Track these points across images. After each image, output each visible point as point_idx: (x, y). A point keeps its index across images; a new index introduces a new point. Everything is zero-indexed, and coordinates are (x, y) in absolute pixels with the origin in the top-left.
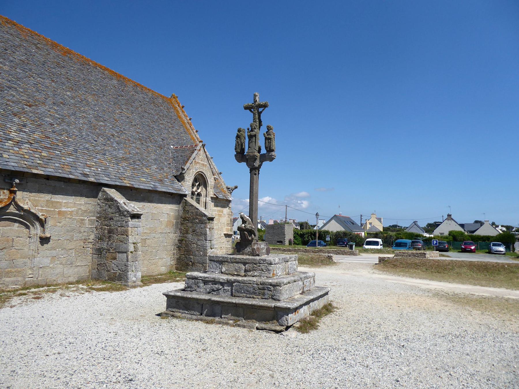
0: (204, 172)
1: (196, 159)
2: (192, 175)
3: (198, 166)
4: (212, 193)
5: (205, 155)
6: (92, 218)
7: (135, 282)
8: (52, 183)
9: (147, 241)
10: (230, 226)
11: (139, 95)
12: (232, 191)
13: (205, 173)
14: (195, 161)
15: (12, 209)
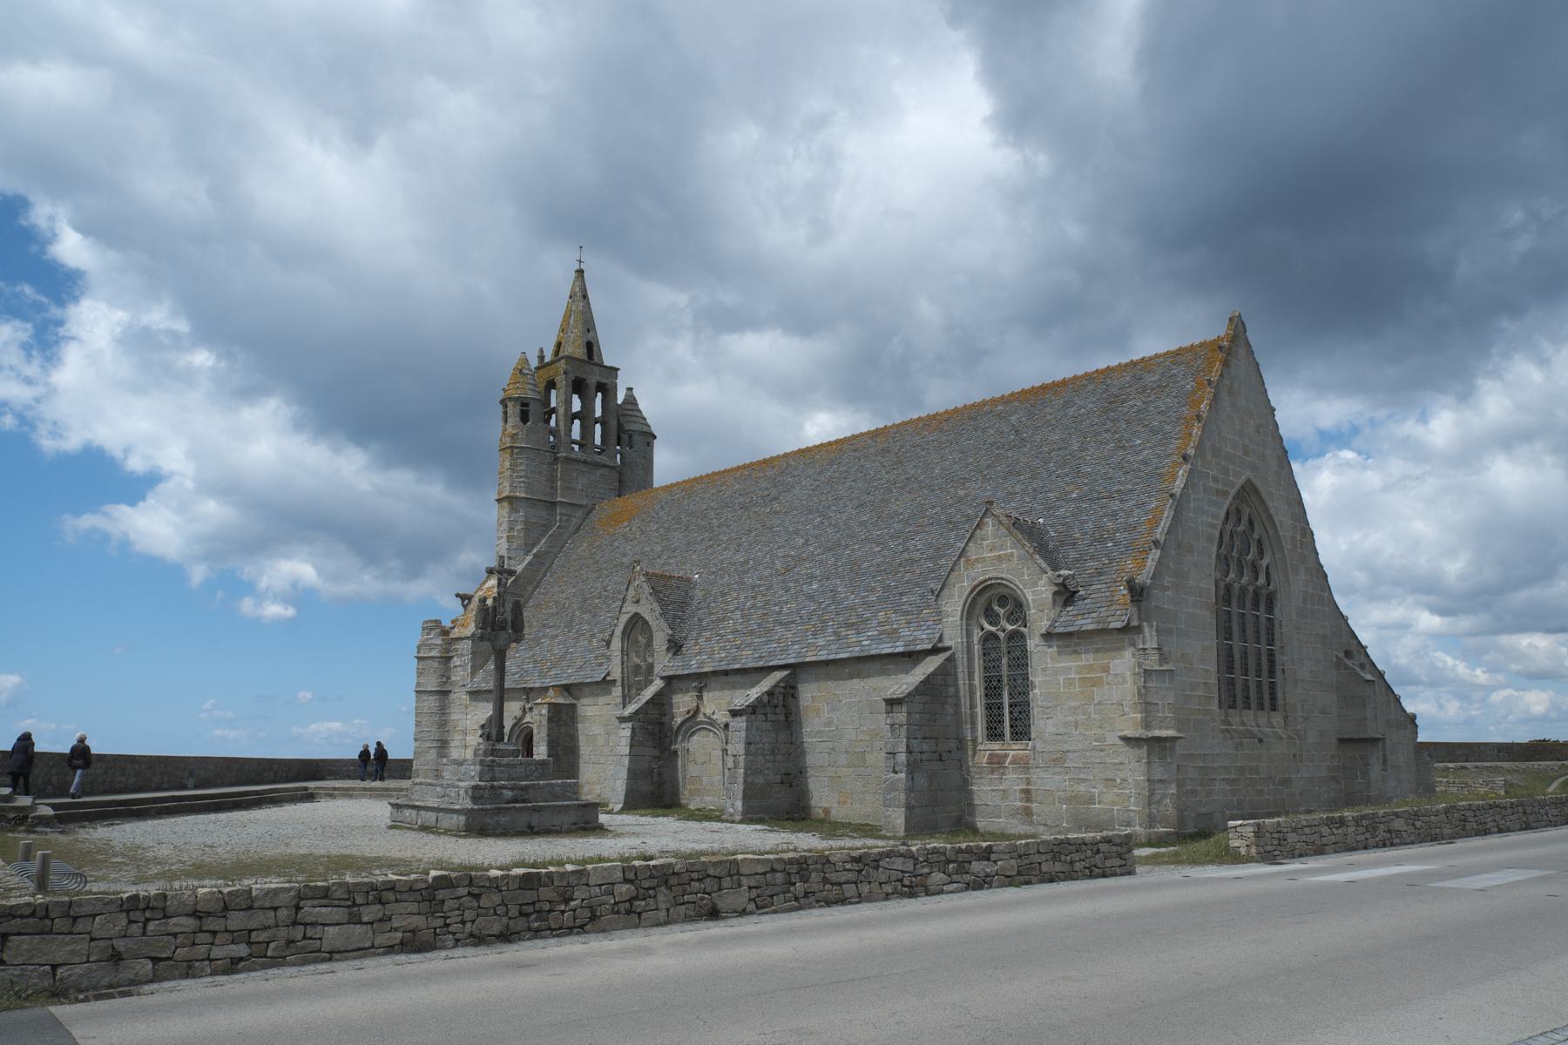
1: (969, 554)
2: (960, 597)
3: (979, 568)
7: (732, 815)
8: (730, 679)
9: (868, 757)
13: (1010, 577)
14: (968, 561)
15: (701, 718)
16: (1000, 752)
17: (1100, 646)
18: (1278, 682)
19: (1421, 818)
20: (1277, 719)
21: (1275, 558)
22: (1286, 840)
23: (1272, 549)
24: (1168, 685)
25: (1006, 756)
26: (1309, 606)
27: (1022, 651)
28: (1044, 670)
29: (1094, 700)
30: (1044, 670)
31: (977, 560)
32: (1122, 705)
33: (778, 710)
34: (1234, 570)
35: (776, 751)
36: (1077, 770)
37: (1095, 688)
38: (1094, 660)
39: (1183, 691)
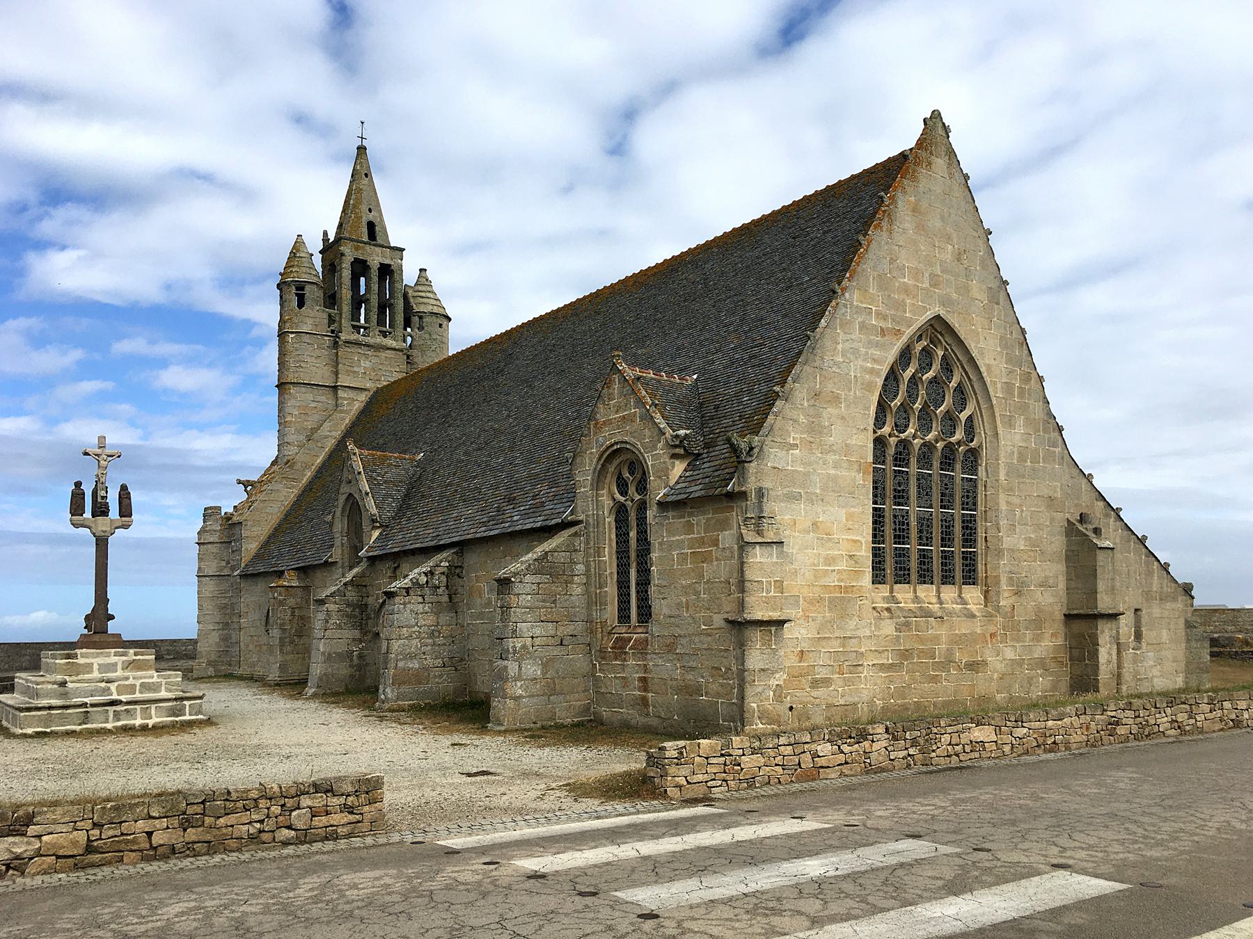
2: (590, 465)
13: (633, 440)
16: (626, 635)
17: (710, 516)
18: (979, 551)
19: (1024, 724)
20: (973, 594)
21: (980, 409)
22: (739, 765)
23: (977, 398)
24: (775, 560)
25: (630, 639)
26: (1029, 464)
28: (660, 544)
33: (440, 591)
34: (914, 424)
35: (436, 634)
36: (687, 658)
37: (705, 565)
38: (705, 533)
39: (814, 565)
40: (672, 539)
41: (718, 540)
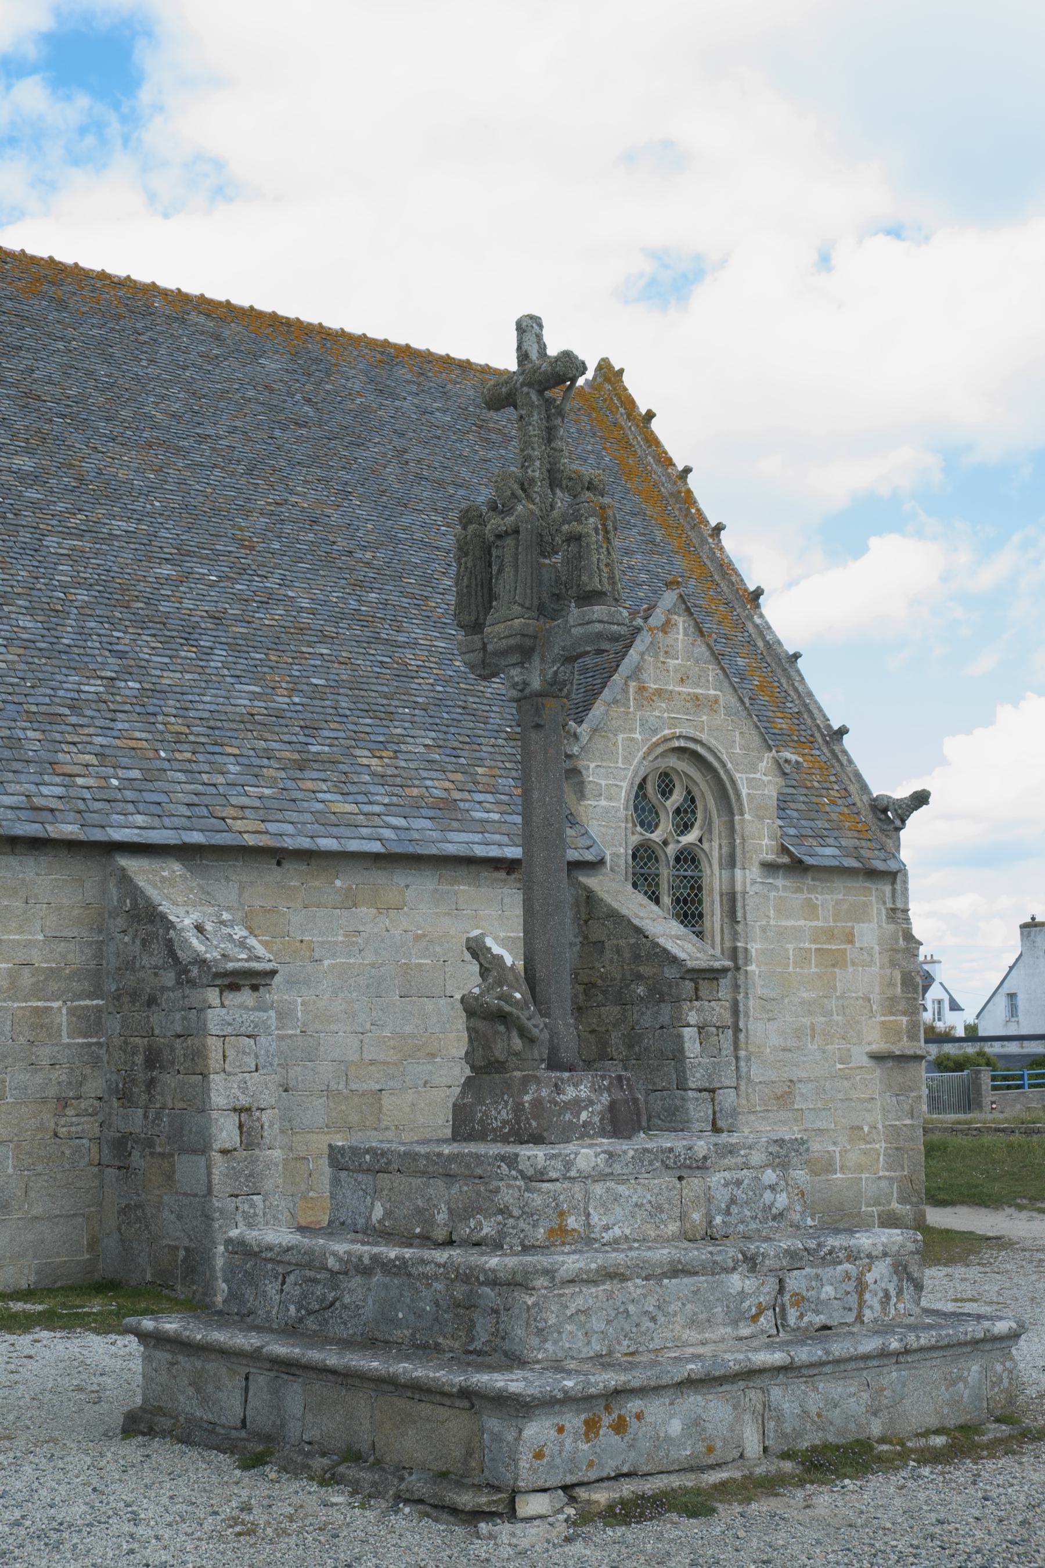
0: (703, 737)
1: (644, 676)
2: (627, 760)
3: (660, 710)
4: (766, 841)
5: (704, 648)
6: (88, 1002)
9: (387, 1101)
10: (904, 1014)
11: (397, 403)
12: (903, 821)
13: (713, 742)
14: (642, 689)
17: (840, 897)
27: (692, 888)
28: (764, 930)
29: (834, 988)
30: (764, 930)
31: (659, 692)
32: (869, 1001)
37: (837, 970)
38: (834, 921)
40: (784, 923)
41: (853, 935)
